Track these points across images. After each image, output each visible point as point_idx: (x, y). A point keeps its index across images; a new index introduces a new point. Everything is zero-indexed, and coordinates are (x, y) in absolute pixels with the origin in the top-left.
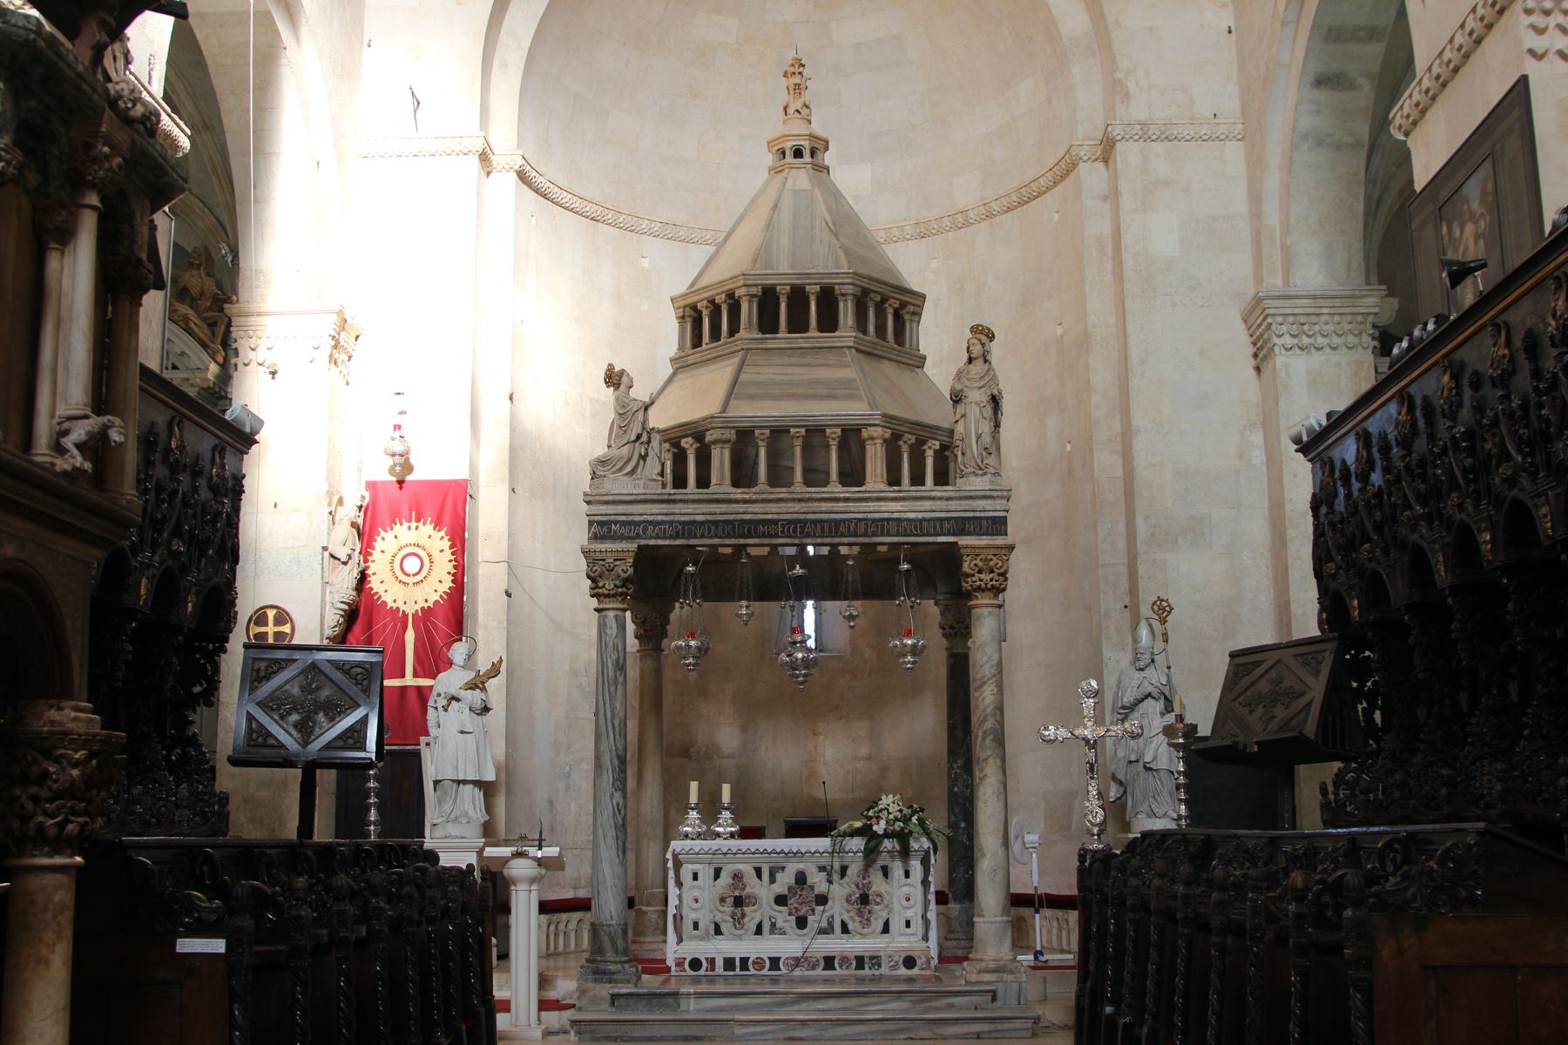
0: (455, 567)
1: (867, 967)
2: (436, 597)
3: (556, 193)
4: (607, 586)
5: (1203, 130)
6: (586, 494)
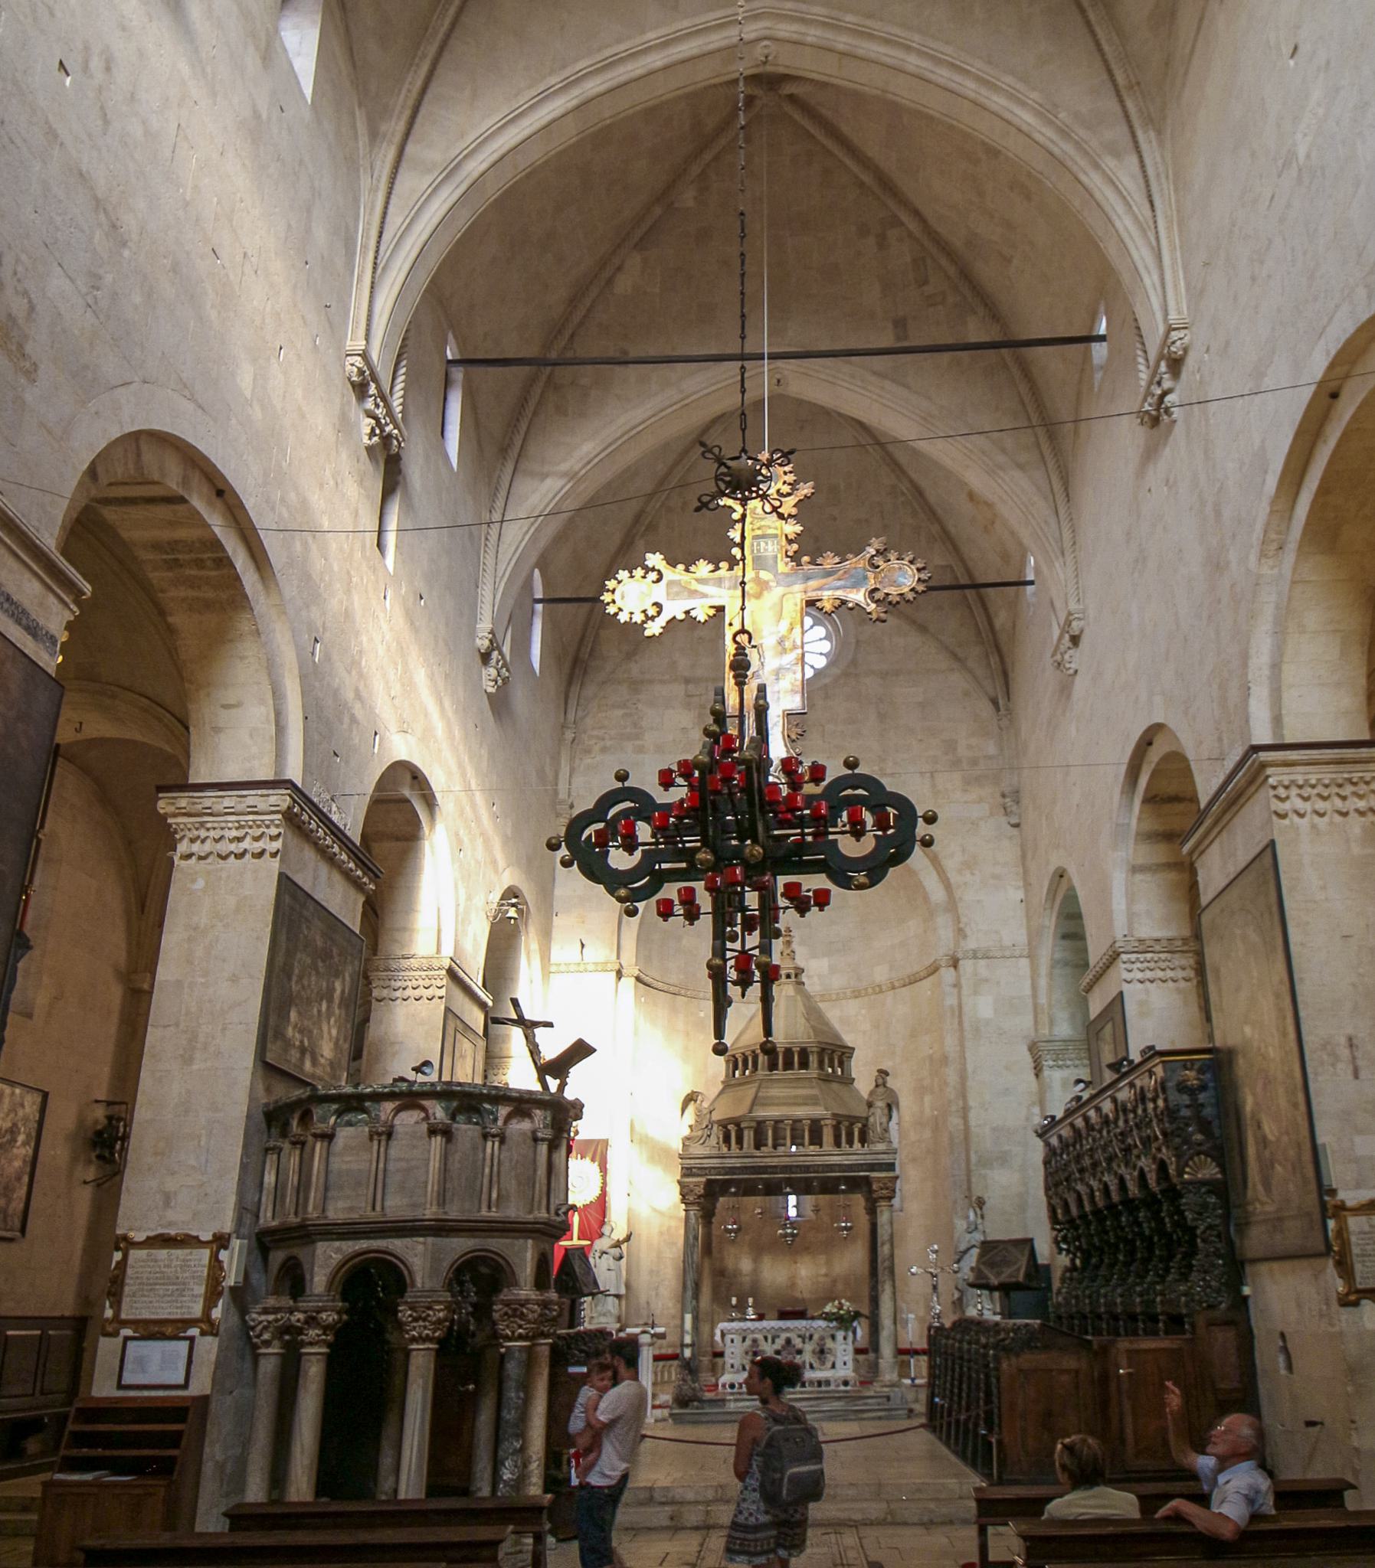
3: (655, 984)
5: (1007, 953)
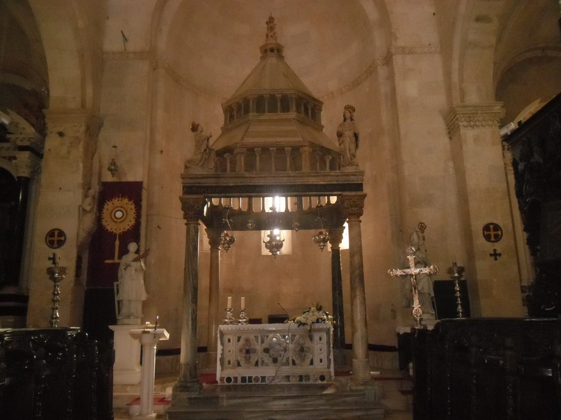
0: (136, 215)
1: (304, 380)
2: (128, 227)
4: (190, 214)
6: (181, 174)
